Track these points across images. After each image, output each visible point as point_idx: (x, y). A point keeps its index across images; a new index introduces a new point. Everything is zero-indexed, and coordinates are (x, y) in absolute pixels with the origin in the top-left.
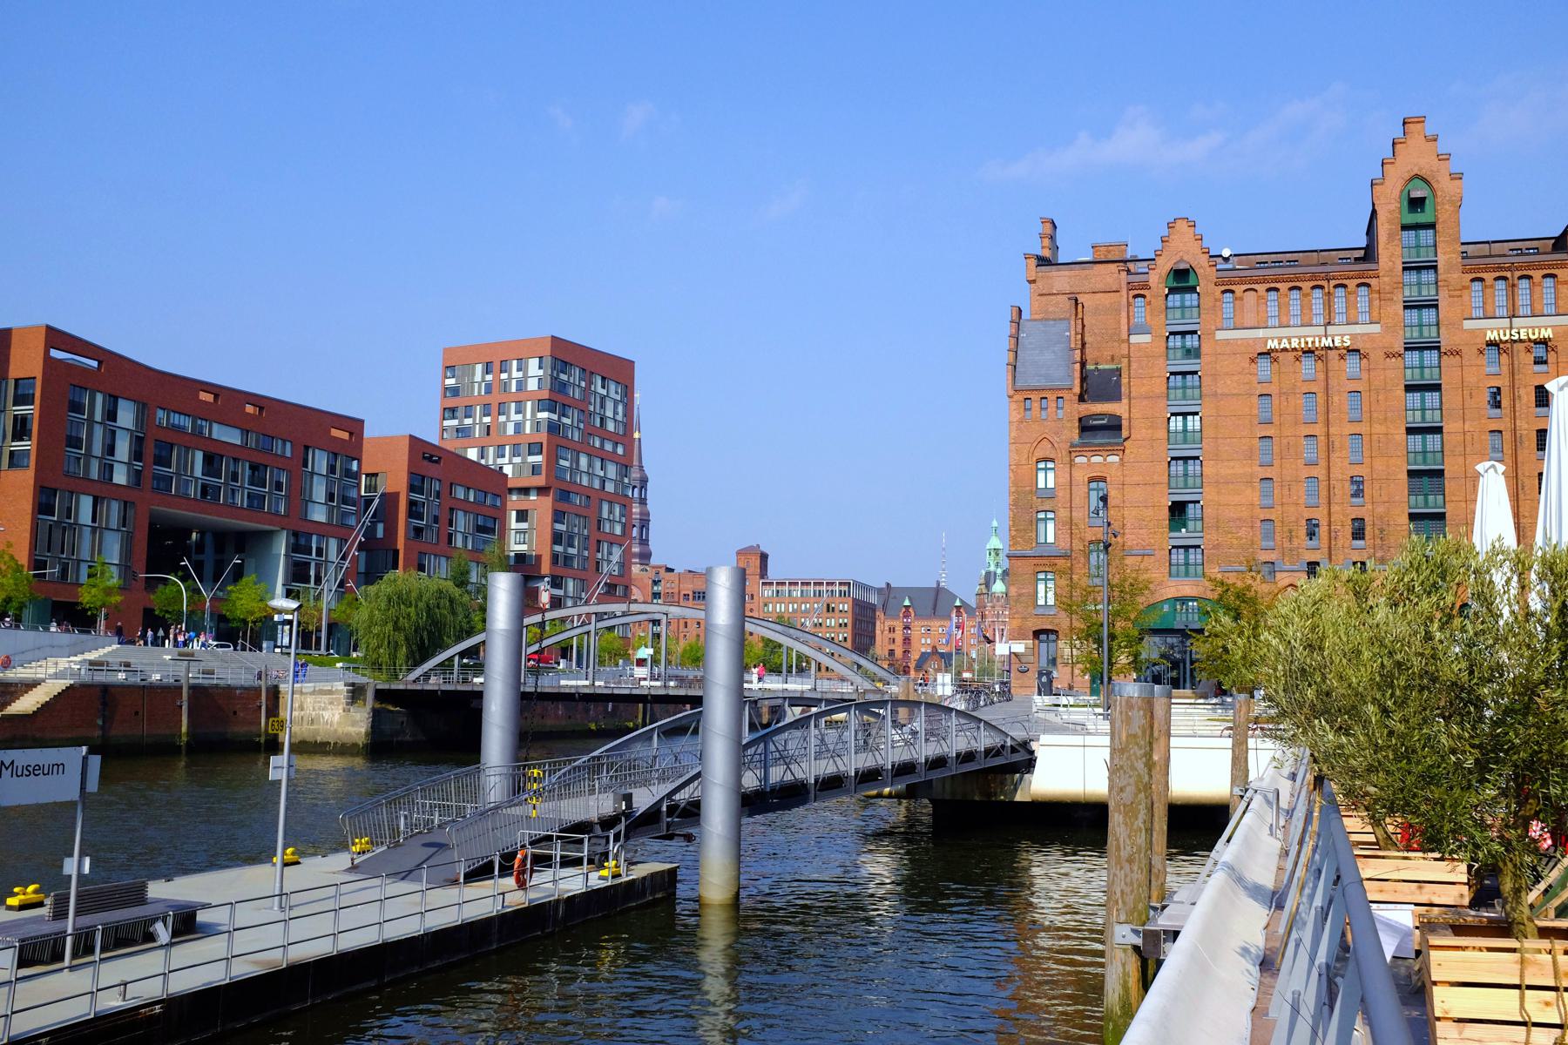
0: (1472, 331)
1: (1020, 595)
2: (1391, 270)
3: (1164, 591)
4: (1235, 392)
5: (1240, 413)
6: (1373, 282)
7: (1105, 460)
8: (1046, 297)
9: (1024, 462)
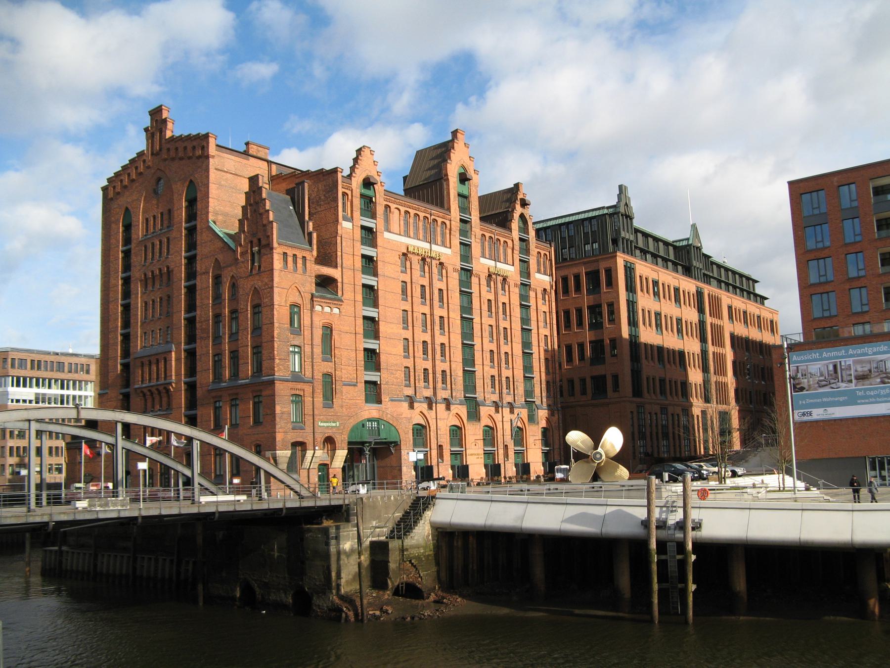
0: (483, 265)
1: (282, 413)
2: (455, 218)
3: (363, 413)
4: (393, 276)
5: (395, 291)
6: (448, 223)
7: (331, 310)
8: (220, 172)
9: (283, 304)
